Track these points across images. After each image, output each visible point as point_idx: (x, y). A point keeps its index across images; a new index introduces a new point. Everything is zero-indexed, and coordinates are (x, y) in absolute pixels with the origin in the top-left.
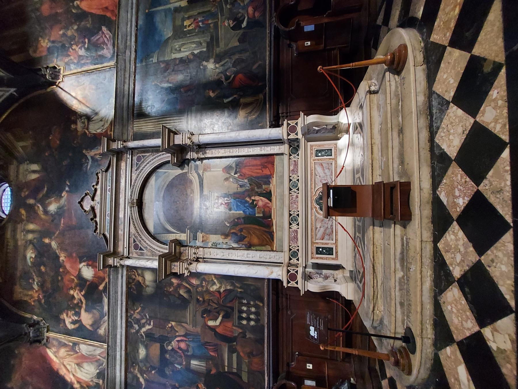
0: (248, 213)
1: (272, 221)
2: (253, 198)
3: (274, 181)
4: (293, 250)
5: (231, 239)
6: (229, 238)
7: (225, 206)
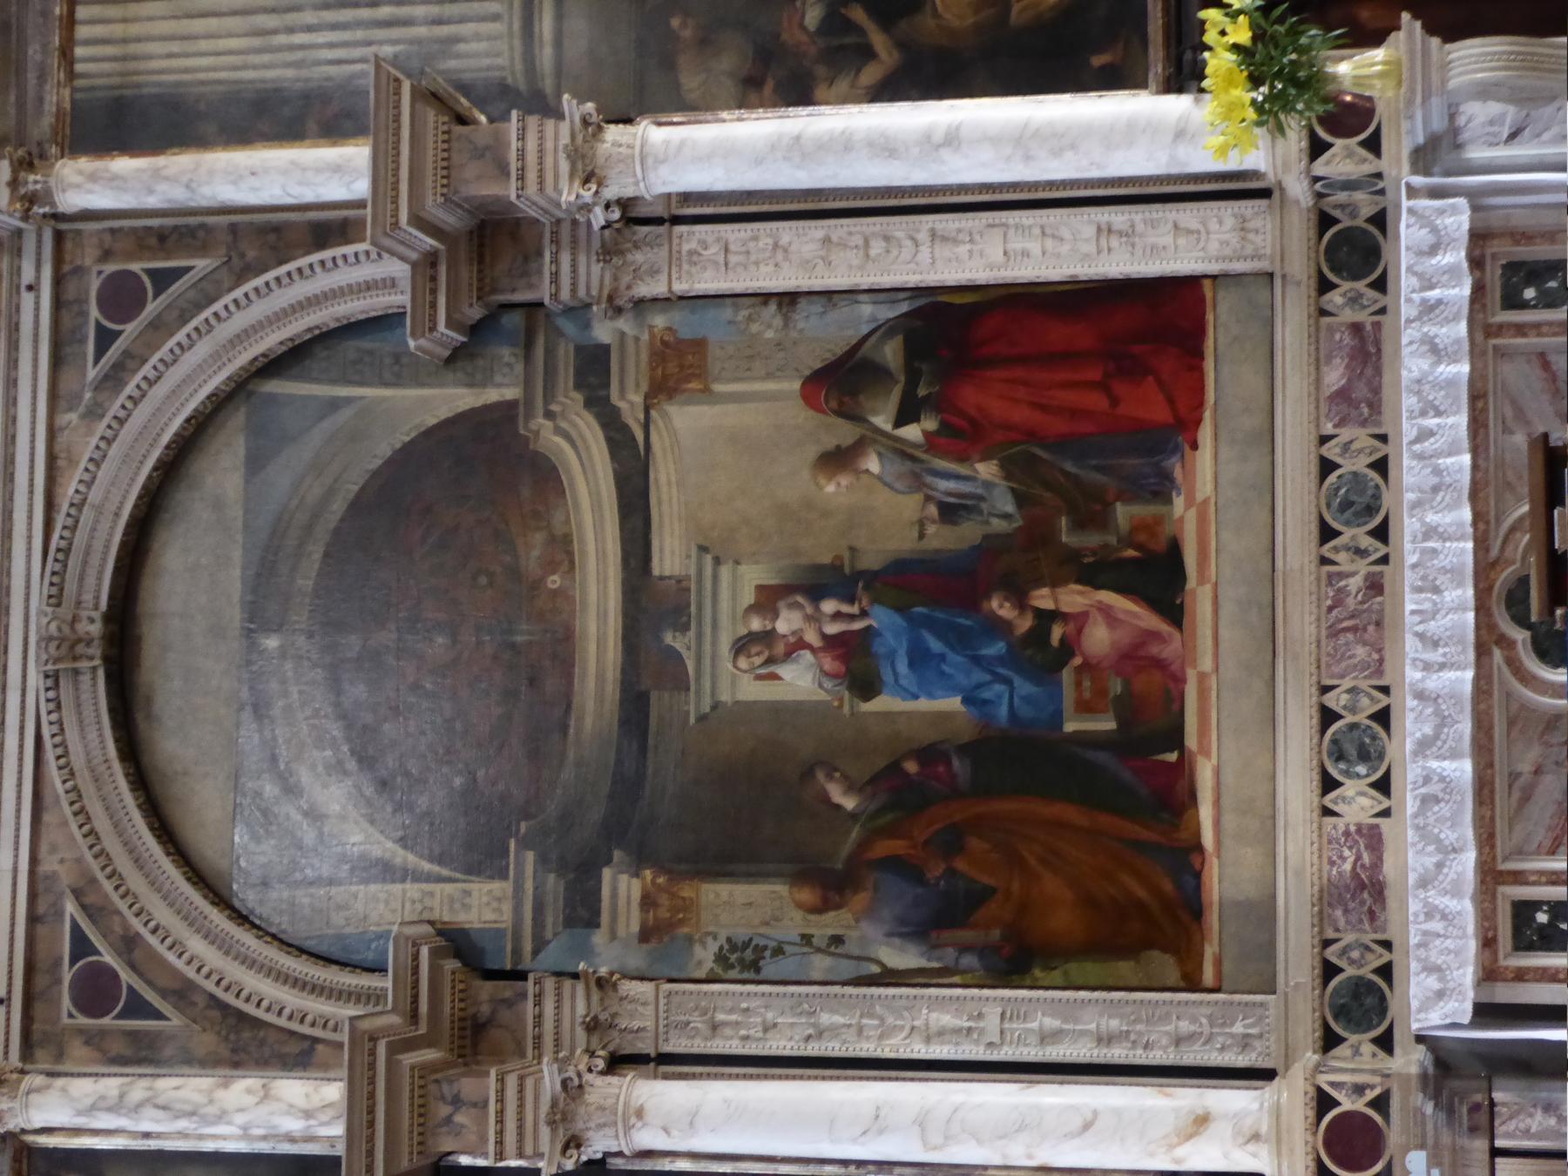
0: (1003, 711)
1: (1183, 771)
2: (1043, 599)
3: (1207, 468)
4: (1350, 971)
5: (870, 913)
6: (861, 899)
7: (829, 664)
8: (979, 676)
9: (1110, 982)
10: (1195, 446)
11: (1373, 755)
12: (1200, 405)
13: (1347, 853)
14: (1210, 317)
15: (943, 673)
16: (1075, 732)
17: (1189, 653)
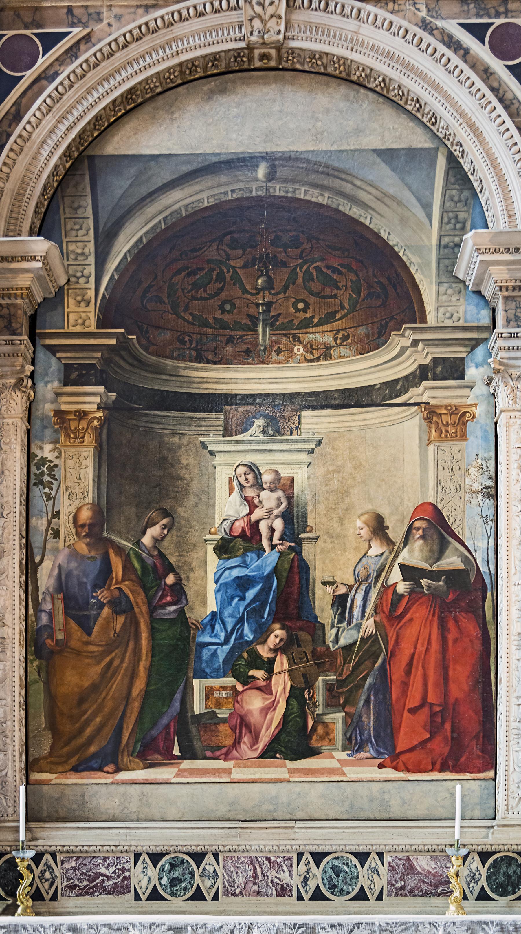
0: (207, 639)
1: (169, 759)
8: (230, 623)
9: (31, 711)
10: (381, 766)
11: (174, 889)
12: (408, 771)
13: (111, 870)
14: (468, 776)
15: (232, 598)
16: (193, 686)
17: (243, 762)
